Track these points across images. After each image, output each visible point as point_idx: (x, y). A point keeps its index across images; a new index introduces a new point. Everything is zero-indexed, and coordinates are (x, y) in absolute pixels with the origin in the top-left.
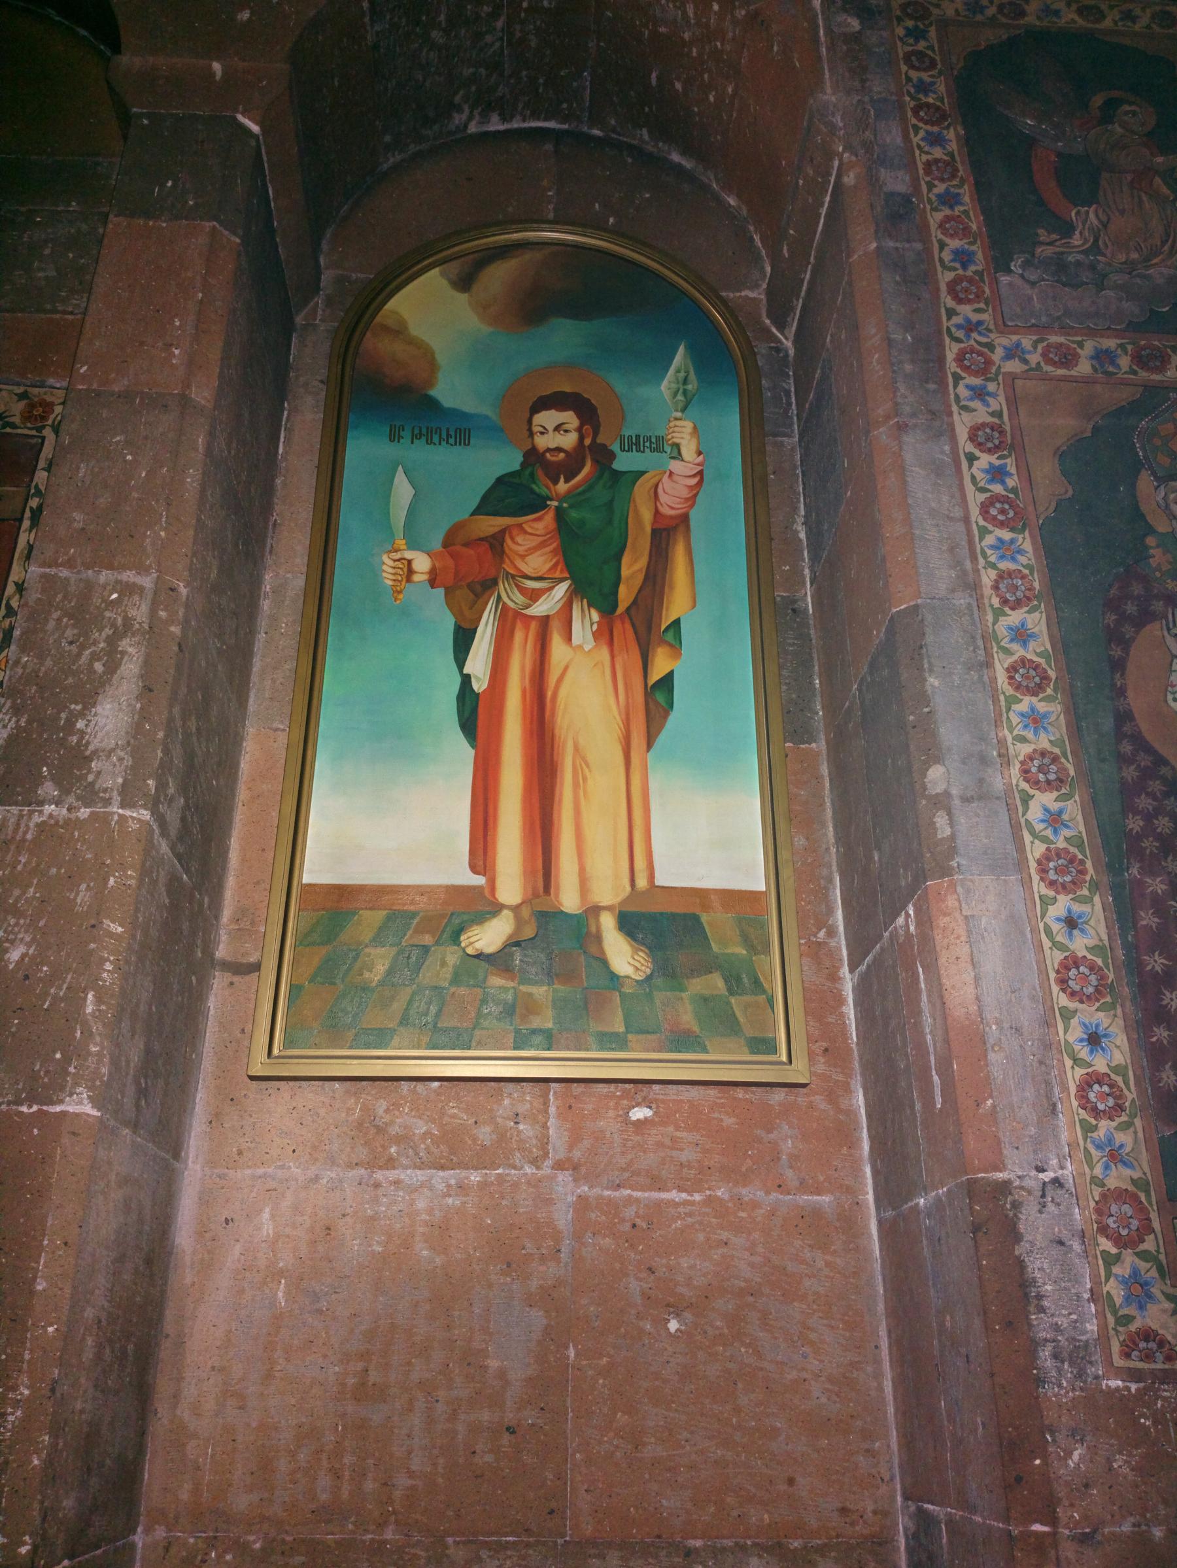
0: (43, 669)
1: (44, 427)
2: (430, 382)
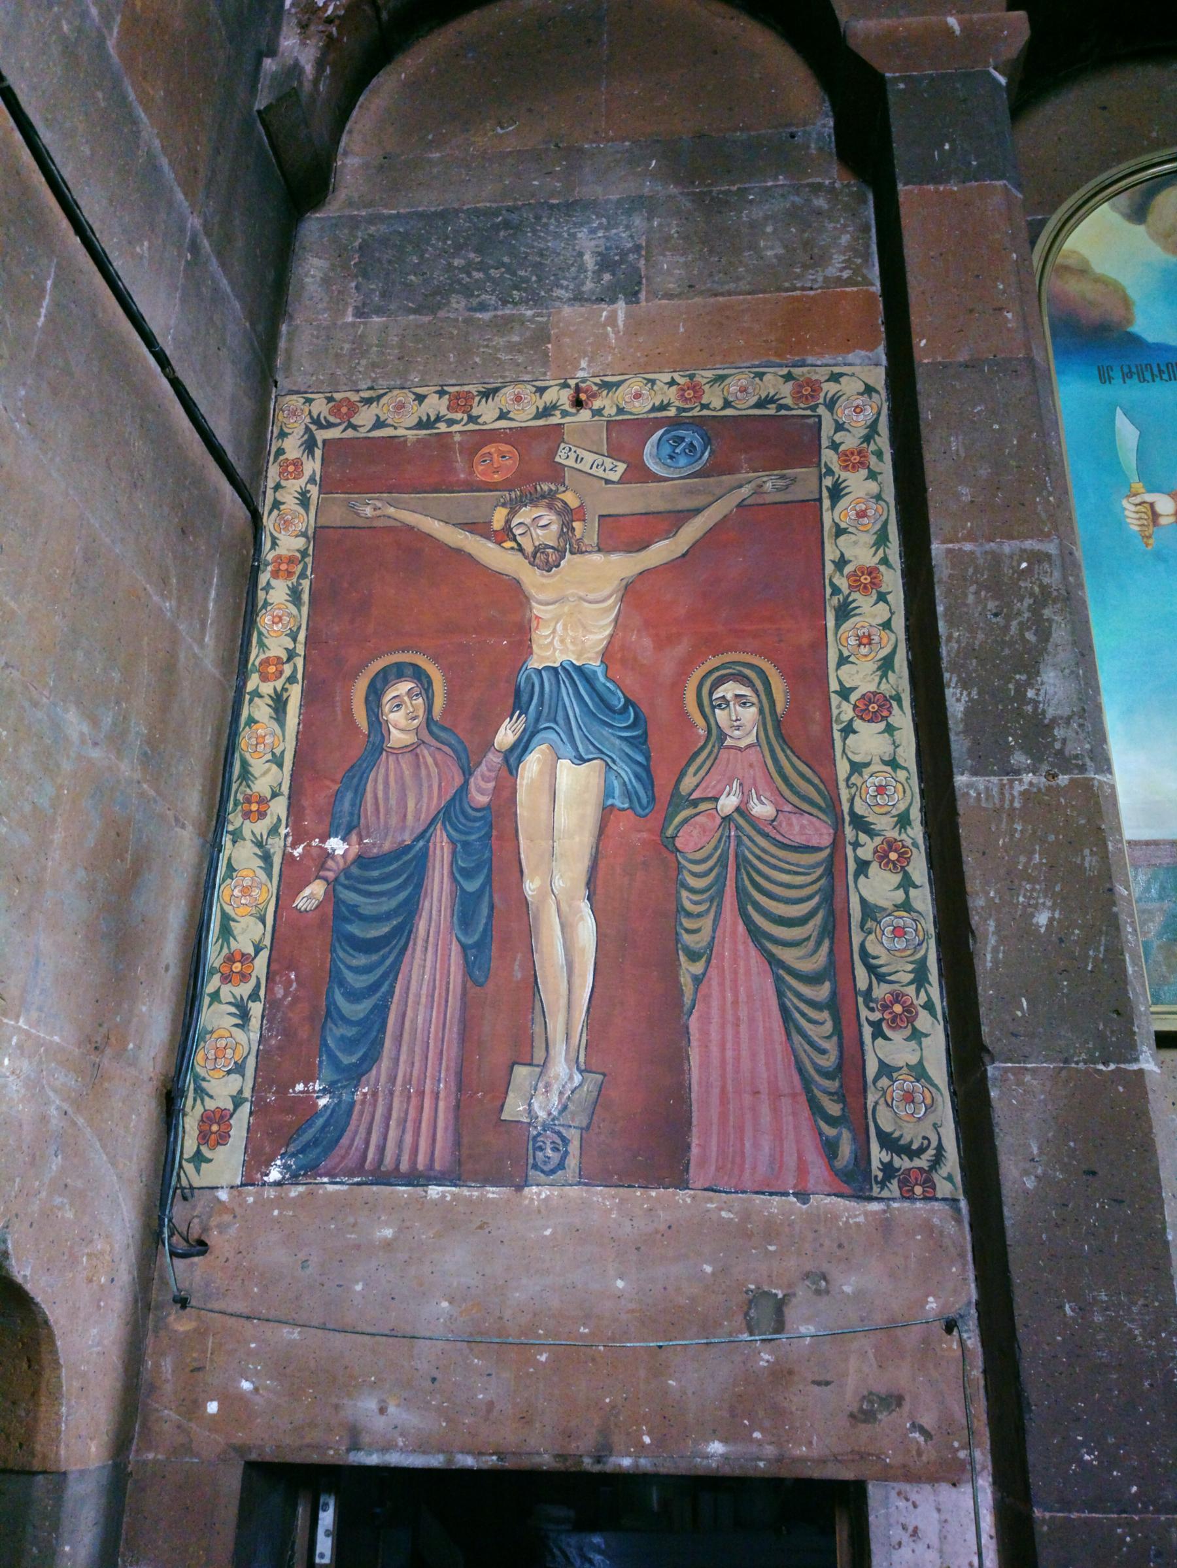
0: (977, 643)
1: (817, 406)
2: (1130, 322)
